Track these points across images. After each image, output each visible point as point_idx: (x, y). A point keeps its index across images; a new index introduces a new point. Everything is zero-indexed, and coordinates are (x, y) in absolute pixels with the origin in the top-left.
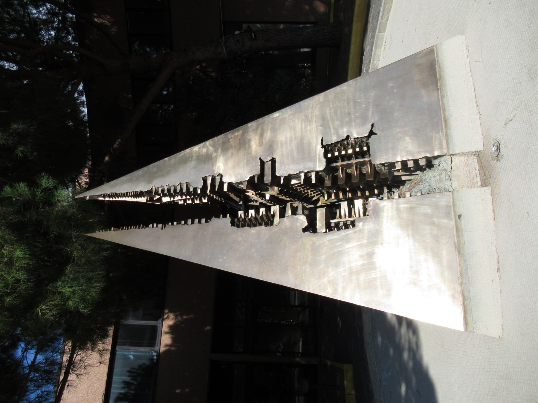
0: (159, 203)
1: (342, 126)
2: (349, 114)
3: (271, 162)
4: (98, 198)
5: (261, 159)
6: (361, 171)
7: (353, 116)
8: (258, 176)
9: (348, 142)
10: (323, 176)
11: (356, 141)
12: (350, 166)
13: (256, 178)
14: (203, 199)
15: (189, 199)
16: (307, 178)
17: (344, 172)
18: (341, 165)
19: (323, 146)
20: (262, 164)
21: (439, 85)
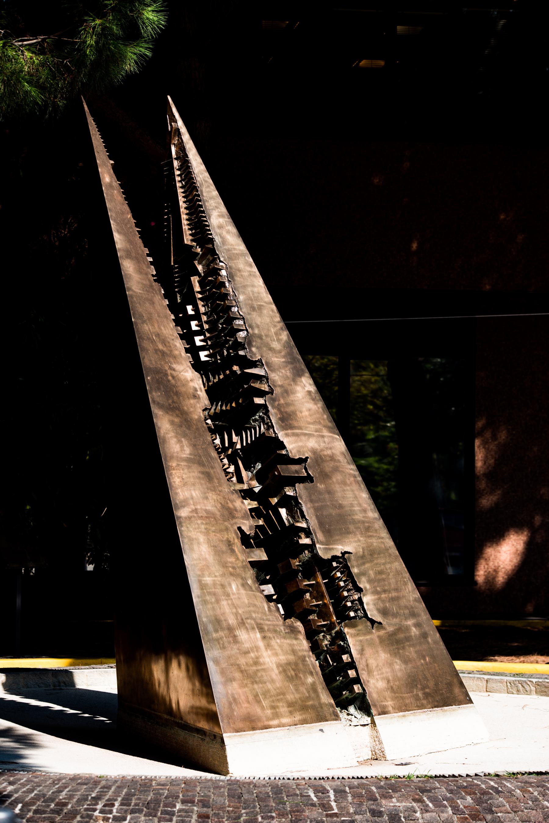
0: (175, 264)
1: (370, 581)
2: (385, 591)
3: (306, 475)
4: (174, 144)
5: (307, 458)
6: (312, 612)
7: (383, 596)
8: (287, 456)
9: (352, 592)
10: (301, 556)
11: (356, 602)
12: (320, 597)
13: (284, 452)
14: (206, 353)
15: (200, 325)
16: (297, 531)
17: (307, 588)
18: (318, 584)
19: (344, 553)
20: (301, 461)
21: (436, 709)
